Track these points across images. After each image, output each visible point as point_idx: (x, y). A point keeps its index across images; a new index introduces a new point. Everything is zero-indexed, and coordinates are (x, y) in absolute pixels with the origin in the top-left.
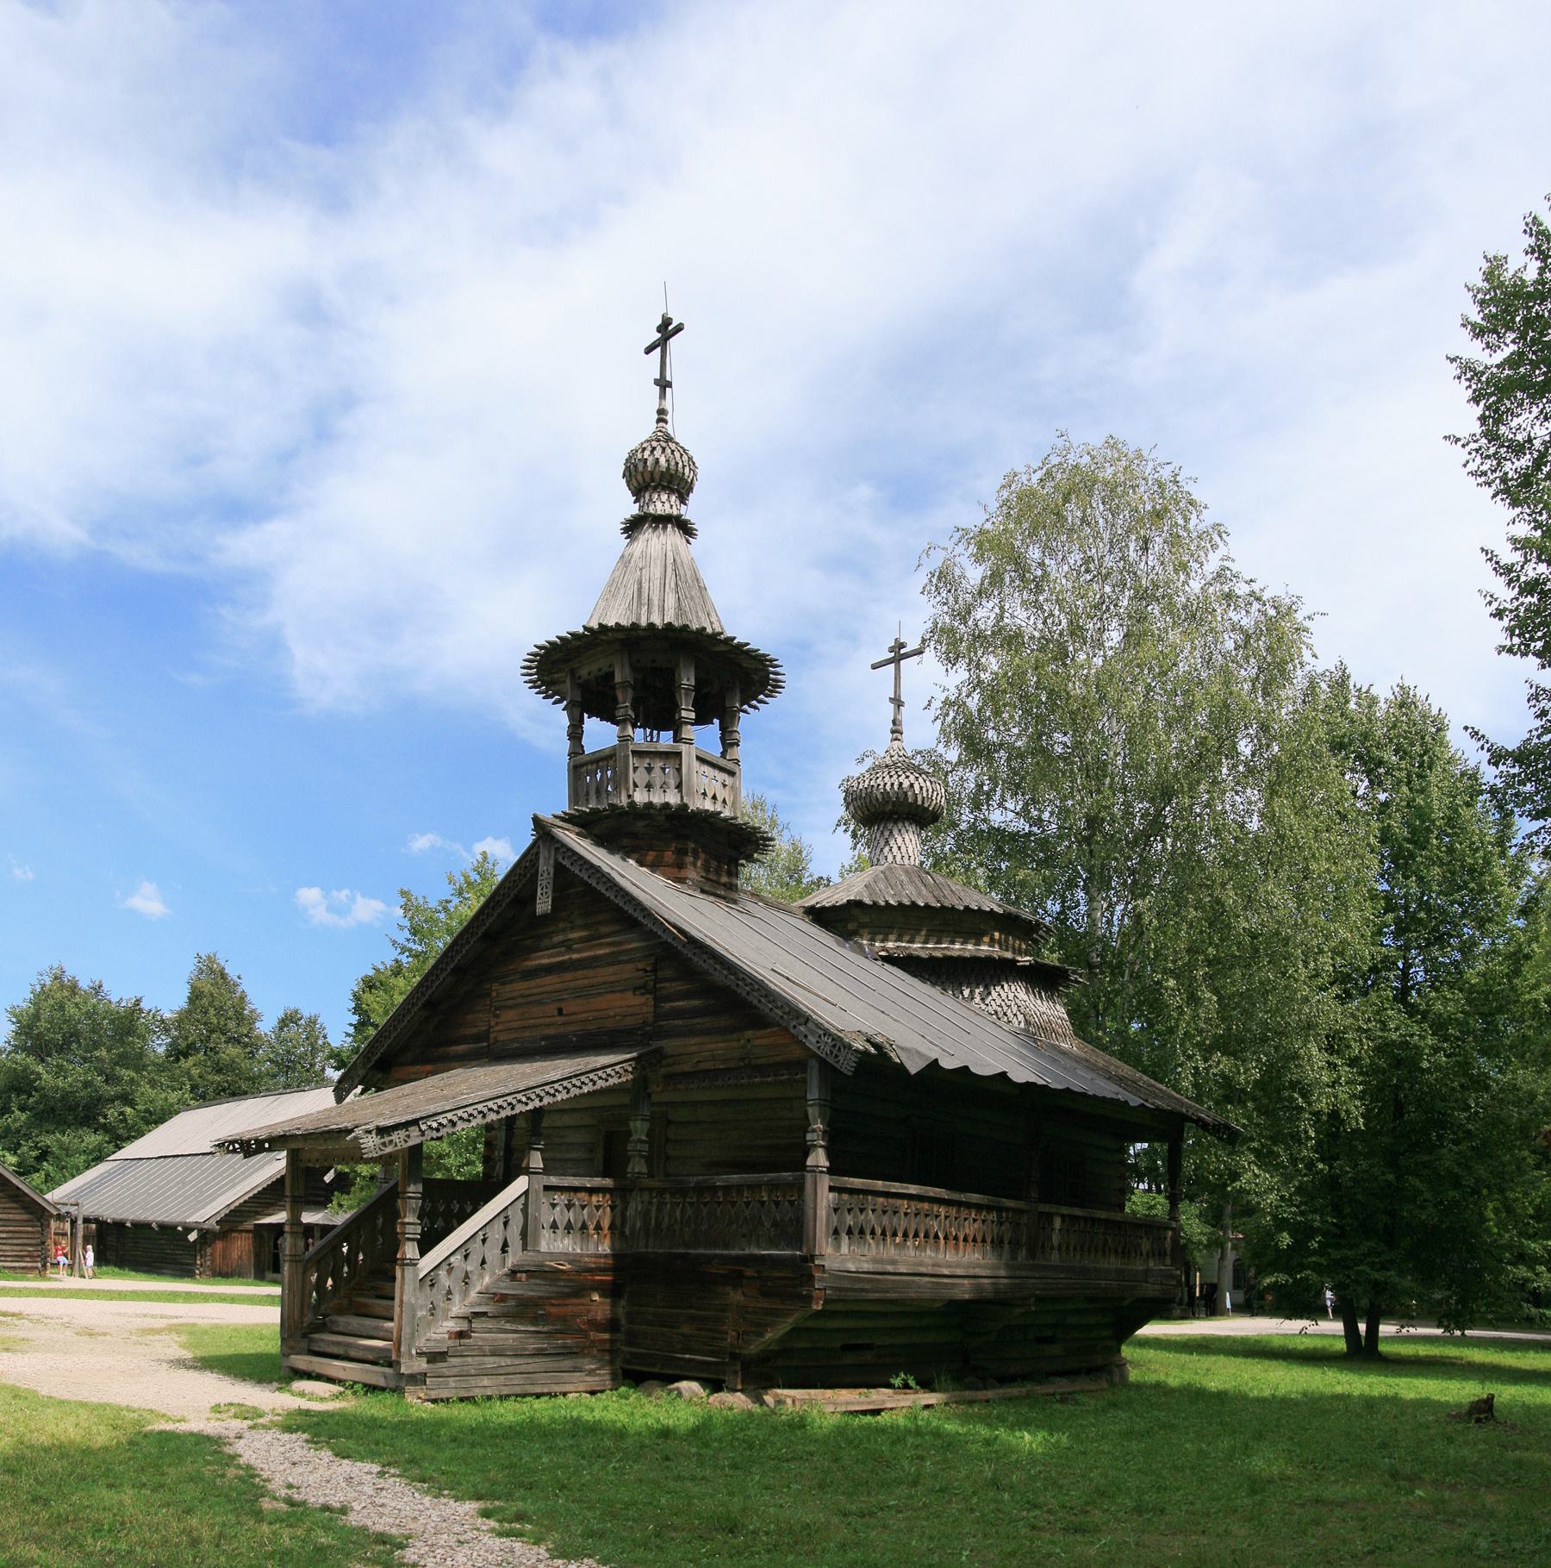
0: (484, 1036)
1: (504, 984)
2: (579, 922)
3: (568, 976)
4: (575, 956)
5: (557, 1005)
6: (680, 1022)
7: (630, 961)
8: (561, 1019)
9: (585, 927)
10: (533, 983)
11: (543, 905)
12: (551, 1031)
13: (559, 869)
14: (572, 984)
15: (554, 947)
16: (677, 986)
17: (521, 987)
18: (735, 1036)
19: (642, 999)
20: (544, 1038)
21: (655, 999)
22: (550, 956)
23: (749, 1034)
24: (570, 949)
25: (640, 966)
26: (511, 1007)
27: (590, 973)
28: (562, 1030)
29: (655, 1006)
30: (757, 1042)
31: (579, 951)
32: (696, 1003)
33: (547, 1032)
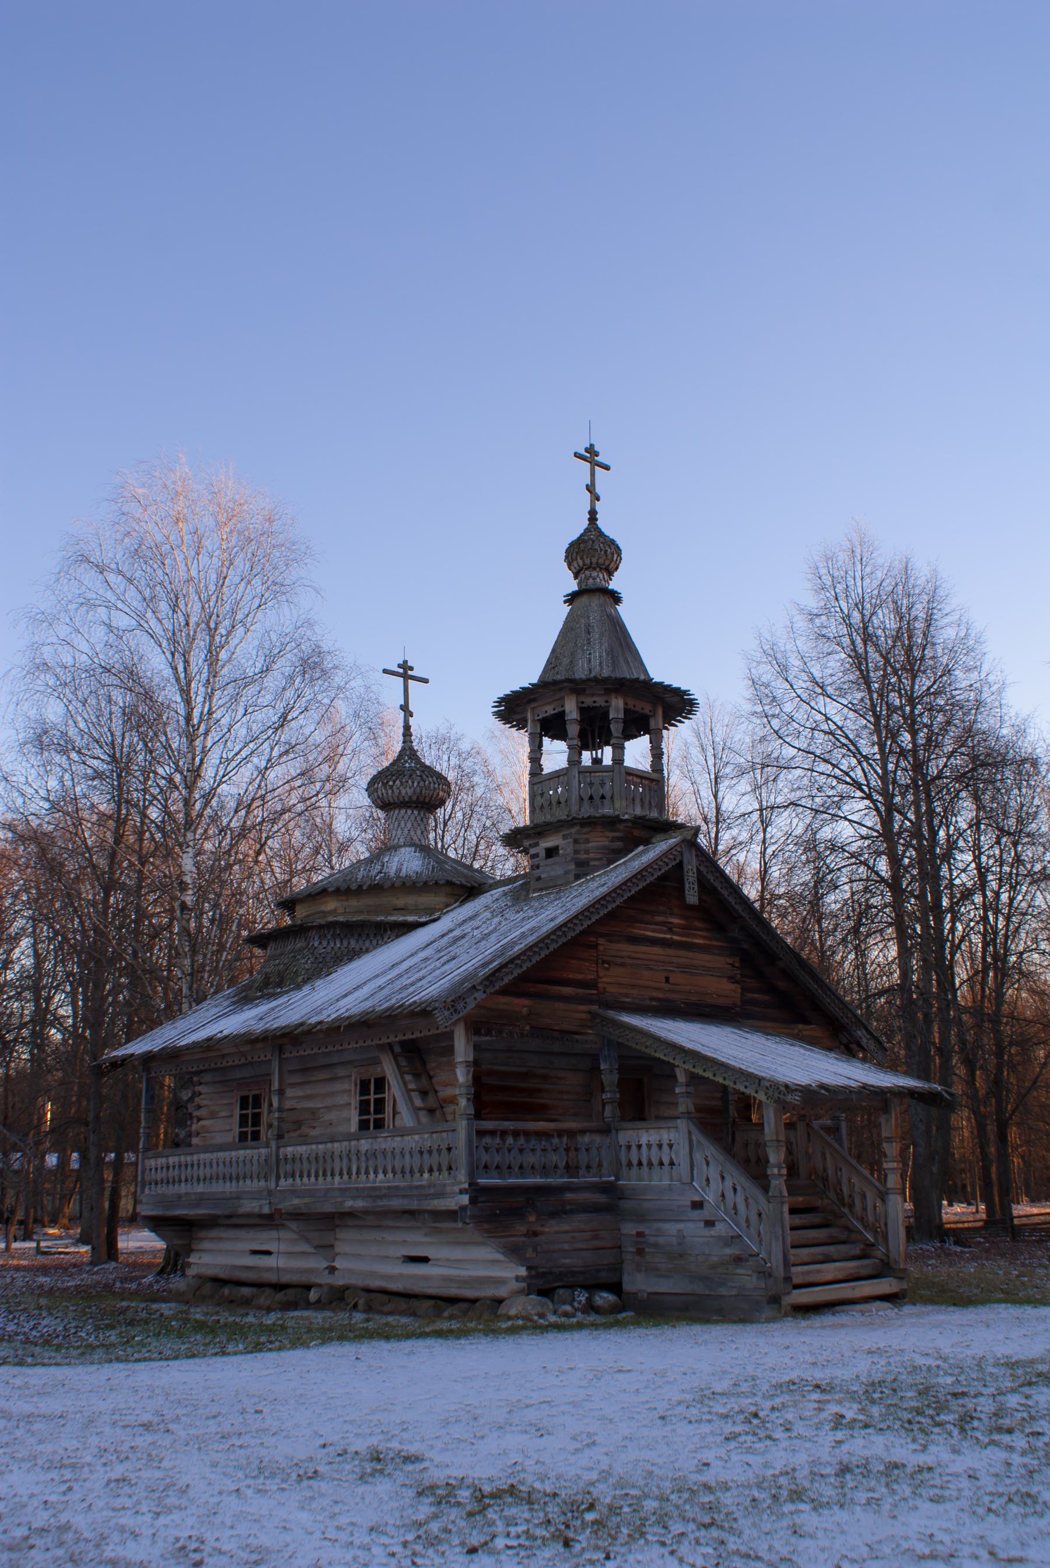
0: (593, 984)
1: (610, 941)
2: (676, 911)
3: (671, 952)
4: (675, 937)
5: (666, 974)
6: (758, 1009)
8: (667, 986)
9: (682, 917)
10: (643, 949)
11: (692, 897)
12: (660, 995)
14: (675, 960)
15: (656, 924)
17: (627, 949)
19: (733, 986)
20: (652, 999)
21: (742, 989)
22: (654, 931)
23: (800, 1026)
24: (670, 931)
26: (623, 965)
27: (690, 954)
29: (742, 994)
30: (805, 1033)
31: (678, 935)
33: (655, 994)
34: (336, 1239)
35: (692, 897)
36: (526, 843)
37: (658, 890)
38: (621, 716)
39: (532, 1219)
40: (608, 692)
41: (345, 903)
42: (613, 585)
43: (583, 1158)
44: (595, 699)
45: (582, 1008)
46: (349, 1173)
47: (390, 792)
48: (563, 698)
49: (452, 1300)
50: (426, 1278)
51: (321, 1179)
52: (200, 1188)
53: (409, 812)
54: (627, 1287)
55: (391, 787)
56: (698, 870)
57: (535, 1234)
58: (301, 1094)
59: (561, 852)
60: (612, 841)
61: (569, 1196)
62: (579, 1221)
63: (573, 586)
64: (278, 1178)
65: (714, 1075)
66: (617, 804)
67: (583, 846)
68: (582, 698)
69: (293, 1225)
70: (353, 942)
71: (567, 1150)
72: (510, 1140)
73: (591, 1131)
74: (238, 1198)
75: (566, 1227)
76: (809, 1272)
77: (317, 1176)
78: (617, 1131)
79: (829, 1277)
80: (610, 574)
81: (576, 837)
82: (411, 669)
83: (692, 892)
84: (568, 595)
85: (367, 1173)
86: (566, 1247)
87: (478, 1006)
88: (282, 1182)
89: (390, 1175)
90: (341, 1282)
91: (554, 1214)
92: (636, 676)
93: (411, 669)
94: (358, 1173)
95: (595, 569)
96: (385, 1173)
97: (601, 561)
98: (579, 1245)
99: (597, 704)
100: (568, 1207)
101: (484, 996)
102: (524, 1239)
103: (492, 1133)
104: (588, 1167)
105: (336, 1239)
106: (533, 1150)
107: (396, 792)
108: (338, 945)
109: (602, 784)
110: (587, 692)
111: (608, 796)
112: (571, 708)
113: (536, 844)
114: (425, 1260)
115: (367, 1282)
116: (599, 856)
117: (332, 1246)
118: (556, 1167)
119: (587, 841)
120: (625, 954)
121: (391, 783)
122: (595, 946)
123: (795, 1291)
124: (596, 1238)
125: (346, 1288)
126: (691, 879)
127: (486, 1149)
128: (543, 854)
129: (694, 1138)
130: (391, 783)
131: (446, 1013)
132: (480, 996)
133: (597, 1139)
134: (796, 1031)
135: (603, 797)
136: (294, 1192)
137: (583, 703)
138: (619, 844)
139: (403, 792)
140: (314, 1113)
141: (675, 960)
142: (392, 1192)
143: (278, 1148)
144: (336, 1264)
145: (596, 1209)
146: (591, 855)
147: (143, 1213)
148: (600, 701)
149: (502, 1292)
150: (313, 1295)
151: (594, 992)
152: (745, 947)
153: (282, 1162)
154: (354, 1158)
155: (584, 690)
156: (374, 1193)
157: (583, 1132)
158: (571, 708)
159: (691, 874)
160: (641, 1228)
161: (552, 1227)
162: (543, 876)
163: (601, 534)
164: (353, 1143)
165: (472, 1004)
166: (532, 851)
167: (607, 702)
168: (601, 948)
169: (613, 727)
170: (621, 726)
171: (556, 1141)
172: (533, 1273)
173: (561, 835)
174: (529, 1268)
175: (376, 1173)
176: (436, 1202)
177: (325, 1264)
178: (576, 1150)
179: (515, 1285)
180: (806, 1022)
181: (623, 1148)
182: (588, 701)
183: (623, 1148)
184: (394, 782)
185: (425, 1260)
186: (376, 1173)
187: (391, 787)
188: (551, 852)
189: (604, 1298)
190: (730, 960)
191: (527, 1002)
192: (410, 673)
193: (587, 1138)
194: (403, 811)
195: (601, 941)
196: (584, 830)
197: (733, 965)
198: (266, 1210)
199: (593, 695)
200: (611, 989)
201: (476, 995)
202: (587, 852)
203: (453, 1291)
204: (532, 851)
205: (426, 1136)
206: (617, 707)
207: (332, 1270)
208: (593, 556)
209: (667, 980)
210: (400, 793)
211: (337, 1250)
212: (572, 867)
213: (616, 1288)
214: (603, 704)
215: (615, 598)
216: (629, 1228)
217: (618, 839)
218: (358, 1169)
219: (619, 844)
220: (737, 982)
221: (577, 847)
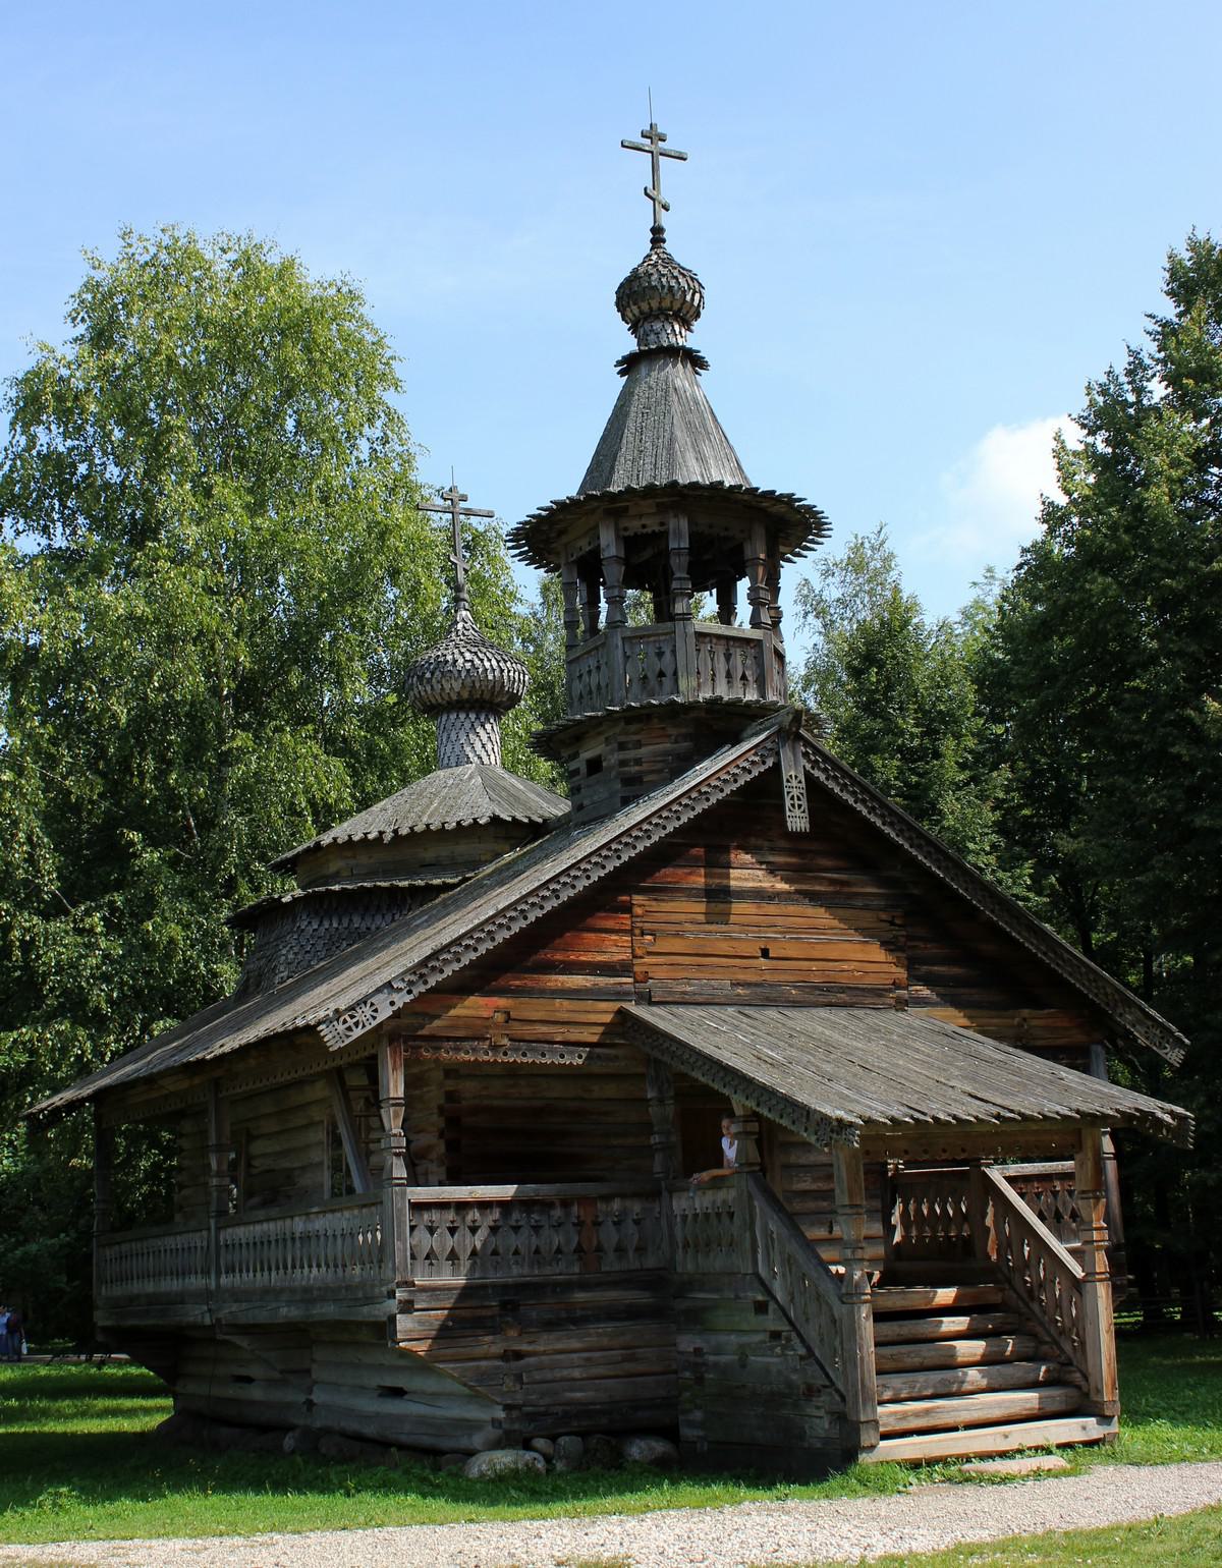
0: (622, 969)
2: (783, 844)
3: (771, 909)
7: (866, 908)
11: (797, 820)
13: (811, 782)
14: (779, 921)
16: (932, 950)
18: (1011, 1012)
20: (736, 984)
21: (908, 959)
23: (1026, 1012)
25: (884, 916)
28: (768, 977)
30: (1035, 1022)
32: (956, 970)
33: (741, 977)
34: (313, 1361)
35: (797, 820)
36: (565, 754)
37: (746, 816)
38: (685, 544)
39: (513, 1333)
40: (662, 509)
41: (352, 862)
42: (691, 339)
43: (609, 1237)
44: (644, 521)
45: (603, 1005)
46: (285, 1268)
47: (428, 688)
48: (596, 527)
49: (434, 1453)
50: (401, 1419)
51: (258, 1274)
52: (150, 1287)
53: (462, 716)
54: (687, 1433)
55: (429, 681)
56: (807, 775)
57: (519, 1356)
58: (278, 1148)
59: (604, 764)
60: (676, 742)
61: (580, 1296)
62: (599, 1333)
63: (631, 344)
64: (218, 1274)
65: (758, 1105)
66: (683, 684)
67: (631, 754)
68: (624, 523)
69: (243, 1342)
70: (357, 922)
71: (580, 1224)
72: (474, 1215)
73: (623, 1196)
74: (182, 1302)
75: (575, 1344)
76: (927, 1412)
77: (255, 1271)
78: (671, 1193)
79: (996, 1414)
80: (687, 324)
81: (622, 739)
82: (464, 499)
83: (797, 812)
84: (619, 363)
85: (302, 1267)
86: (577, 1373)
87: (397, 1015)
88: (224, 1280)
89: (324, 1269)
90: (318, 1424)
91: (550, 1325)
92: (716, 478)
93: (464, 499)
94: (294, 1267)
95: (657, 317)
96: (319, 1266)
97: (666, 304)
98: (600, 1371)
99: (649, 530)
100: (579, 1313)
101: (408, 998)
102: (500, 1363)
103: (443, 1206)
104: (620, 1250)
105: (313, 1361)
106: (516, 1229)
107: (438, 687)
108: (335, 925)
109: (660, 654)
110: (632, 512)
111: (669, 672)
112: (609, 543)
113: (575, 756)
114: (398, 1393)
115: (343, 1424)
116: (659, 766)
117: (308, 1371)
118: (559, 1251)
119: (639, 745)
120: (683, 917)
121: (428, 675)
122: (628, 908)
123: (883, 1443)
124: (631, 1359)
125: (327, 1431)
126: (795, 792)
127: (431, 1230)
128: (584, 769)
129: (756, 1203)
130: (428, 675)
131: (341, 1028)
132: (402, 999)
133: (636, 1207)
134: (1016, 1021)
135: (661, 674)
136: (237, 1295)
137: (626, 529)
138: (686, 745)
139: (447, 686)
140: (289, 1176)
141: (779, 921)
142: (324, 1294)
143: (218, 1229)
144: (314, 1398)
145: (633, 1313)
146: (645, 767)
147: (101, 1323)
148: (652, 525)
149: (477, 1440)
150: (289, 1442)
151: (630, 980)
152: (915, 892)
153: (223, 1250)
154: (289, 1243)
155: (626, 509)
156: (308, 1296)
157: (607, 1198)
158: (609, 543)
159: (794, 783)
160: (699, 1342)
161: (545, 1343)
162: (586, 802)
163: (669, 261)
164: (288, 1222)
165: (385, 1013)
166: (573, 765)
167: (662, 524)
168: (638, 911)
169: (674, 561)
170: (685, 560)
171: (557, 1213)
172: (515, 1414)
173: (602, 738)
174: (507, 1408)
175: (310, 1266)
176: (365, 1309)
177: (302, 1398)
178: (597, 1224)
179: (492, 1433)
180: (1037, 1004)
181: (679, 1219)
182: (634, 526)
183: (679, 1219)
184: (432, 674)
185: (398, 1393)
186: (310, 1266)
187: (429, 681)
188: (594, 766)
189: (637, 1450)
190: (884, 916)
191: (502, 1002)
192: (462, 505)
193: (616, 1205)
194: (453, 716)
195: (637, 899)
196: (633, 728)
197: (892, 923)
198: (207, 1321)
199: (641, 516)
200: (659, 973)
201: (395, 997)
202: (638, 762)
203: (427, 1441)
204: (573, 765)
205: (356, 1212)
206: (679, 533)
207: (310, 1404)
208: (656, 303)
209: (765, 953)
210: (443, 689)
211: (314, 1376)
212: (619, 786)
213: (669, 1432)
214: (657, 529)
215: (696, 361)
216: (687, 1343)
217: (685, 737)
218: (293, 1260)
219: (686, 745)
220: (900, 949)
221: (623, 755)
